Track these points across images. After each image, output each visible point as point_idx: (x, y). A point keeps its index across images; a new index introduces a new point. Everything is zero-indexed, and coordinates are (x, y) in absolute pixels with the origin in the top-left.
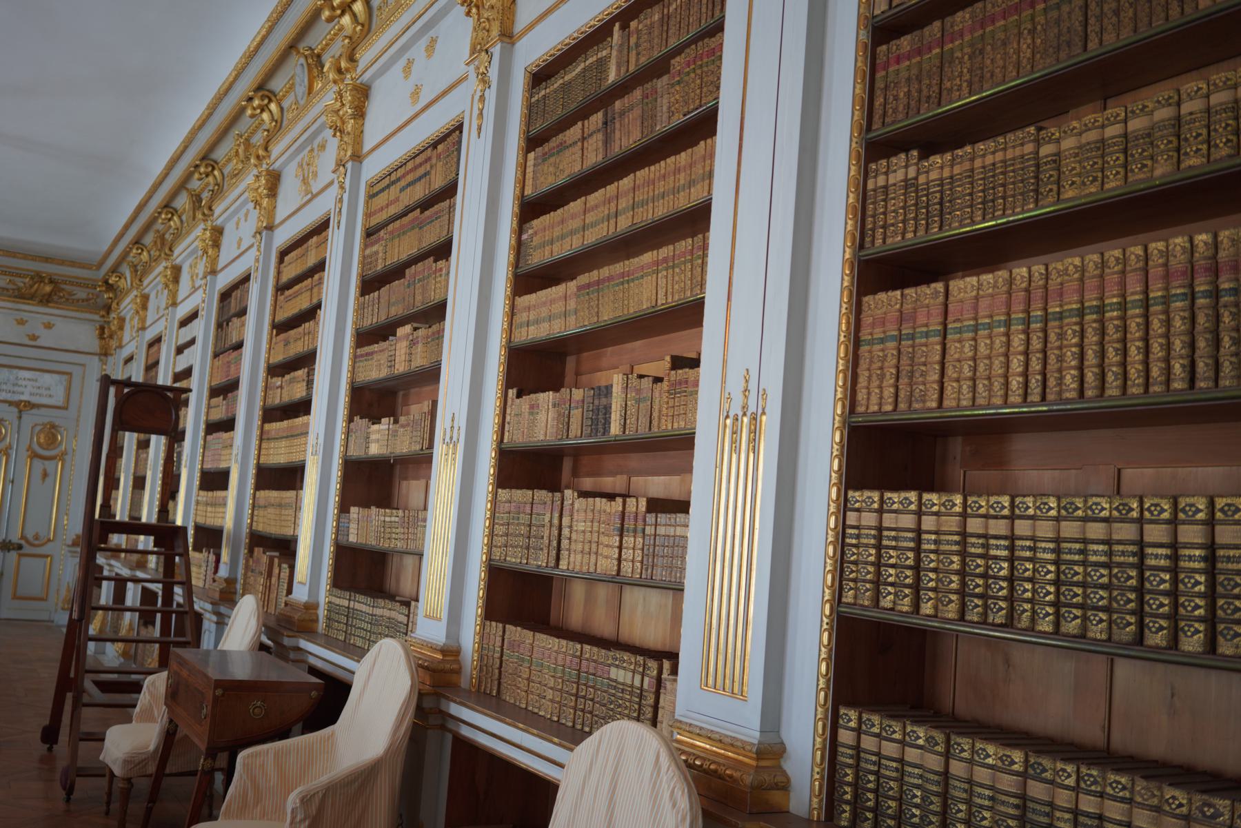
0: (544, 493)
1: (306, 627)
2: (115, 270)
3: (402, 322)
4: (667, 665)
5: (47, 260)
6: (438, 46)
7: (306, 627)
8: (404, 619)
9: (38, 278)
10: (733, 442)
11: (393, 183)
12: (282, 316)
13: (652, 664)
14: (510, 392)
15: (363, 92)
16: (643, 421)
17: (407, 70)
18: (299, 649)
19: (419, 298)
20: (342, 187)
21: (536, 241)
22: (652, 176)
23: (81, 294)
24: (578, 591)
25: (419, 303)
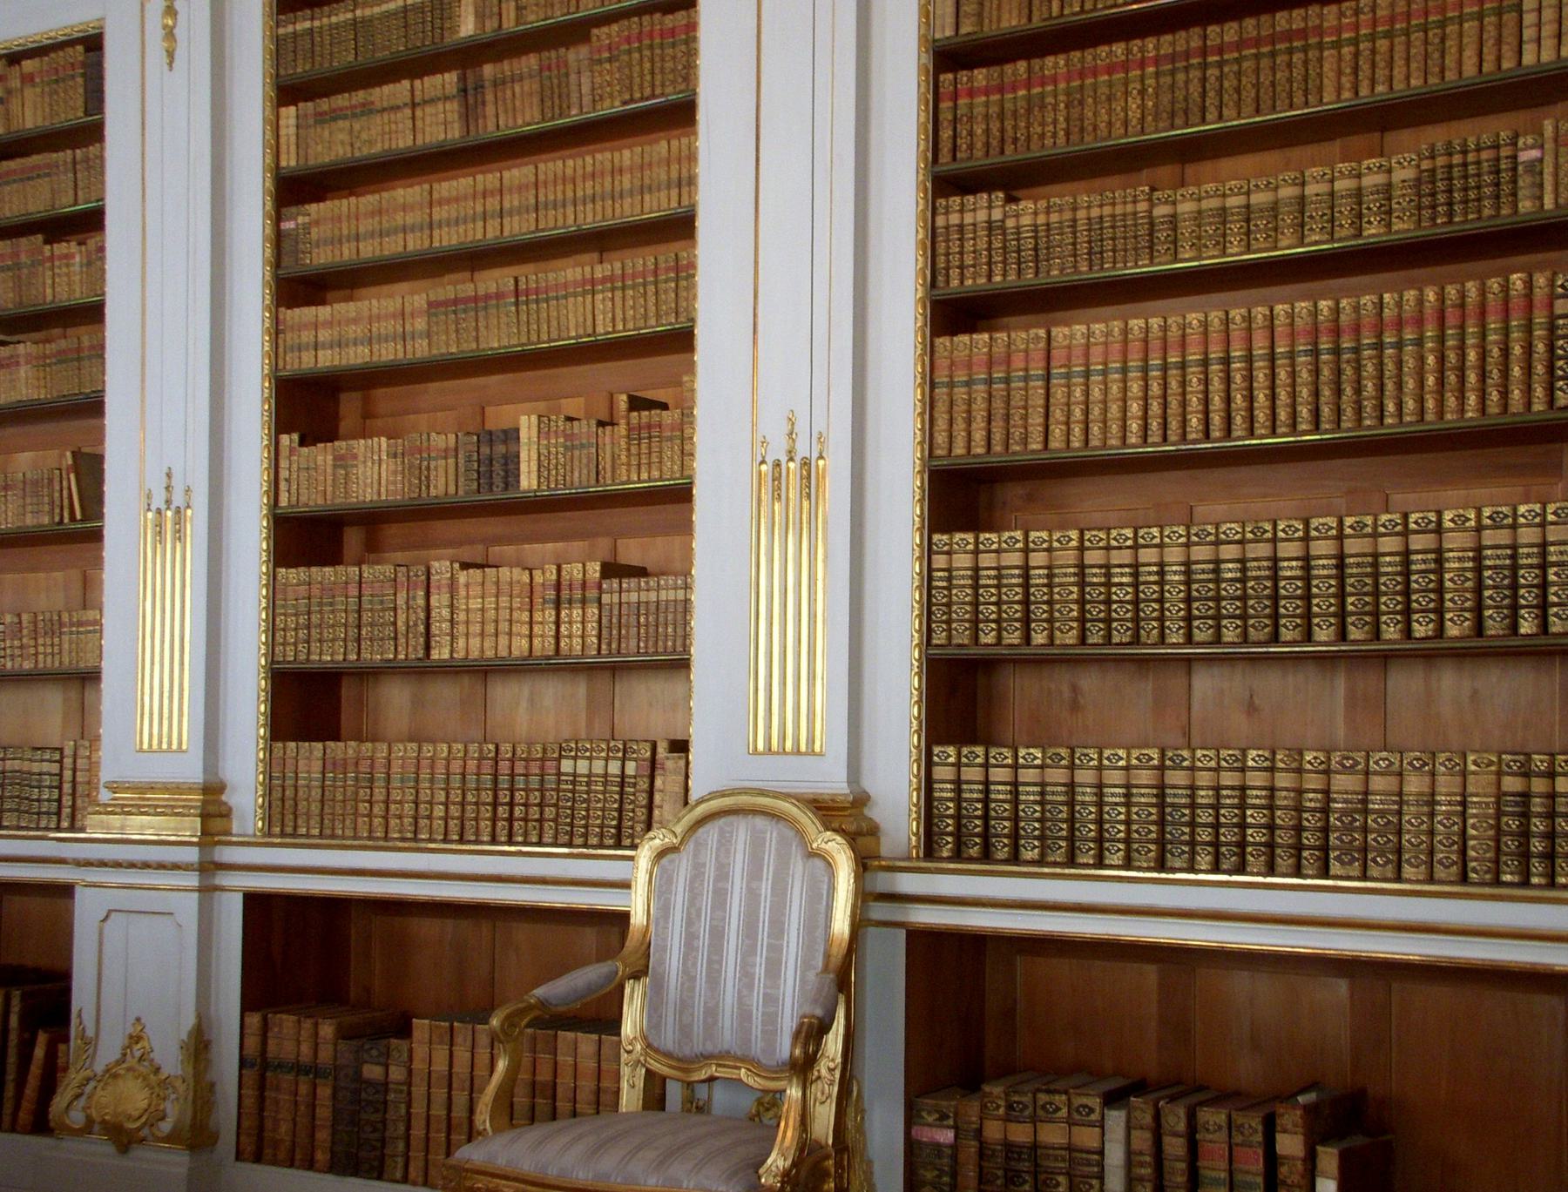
8: (55, 768)
14: (285, 439)
22: (569, 172)
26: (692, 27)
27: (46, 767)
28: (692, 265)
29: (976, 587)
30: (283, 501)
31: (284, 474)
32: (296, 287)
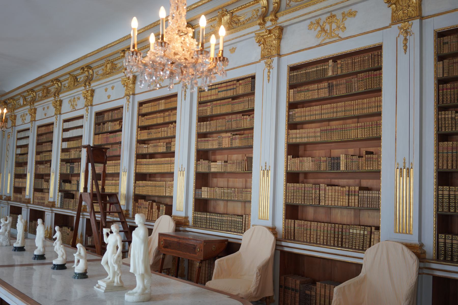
2: (12, 98)
11: (216, 88)
14: (289, 157)
22: (352, 104)
25: (234, 126)
26: (381, 74)
27: (240, 220)
28: (380, 124)
29: (449, 199)
30: (289, 169)
31: (289, 164)
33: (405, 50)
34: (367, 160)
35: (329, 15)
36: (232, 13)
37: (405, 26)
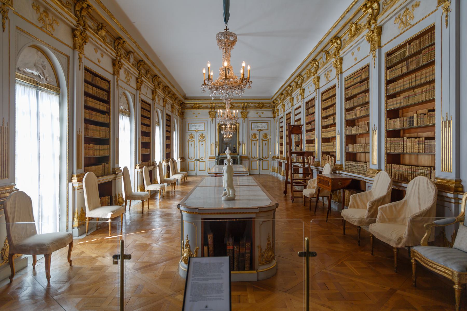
0: (399, 138)
1: (341, 169)
2: (275, 100)
3: (358, 106)
4: (432, 168)
5: (261, 99)
6: (360, 49)
7: (341, 169)
9: (260, 103)
10: (445, 126)
12: (324, 107)
13: (429, 169)
14: (388, 119)
15: (341, 59)
16: (422, 123)
17: (353, 54)
18: (340, 173)
19: (361, 101)
20: (338, 79)
21: (391, 88)
23: (268, 105)
24: (407, 157)
25: (361, 102)
32: (389, 97)
33: (447, 26)
34: (429, 116)
35: (405, 9)
36: (357, 23)
37: (446, 5)
